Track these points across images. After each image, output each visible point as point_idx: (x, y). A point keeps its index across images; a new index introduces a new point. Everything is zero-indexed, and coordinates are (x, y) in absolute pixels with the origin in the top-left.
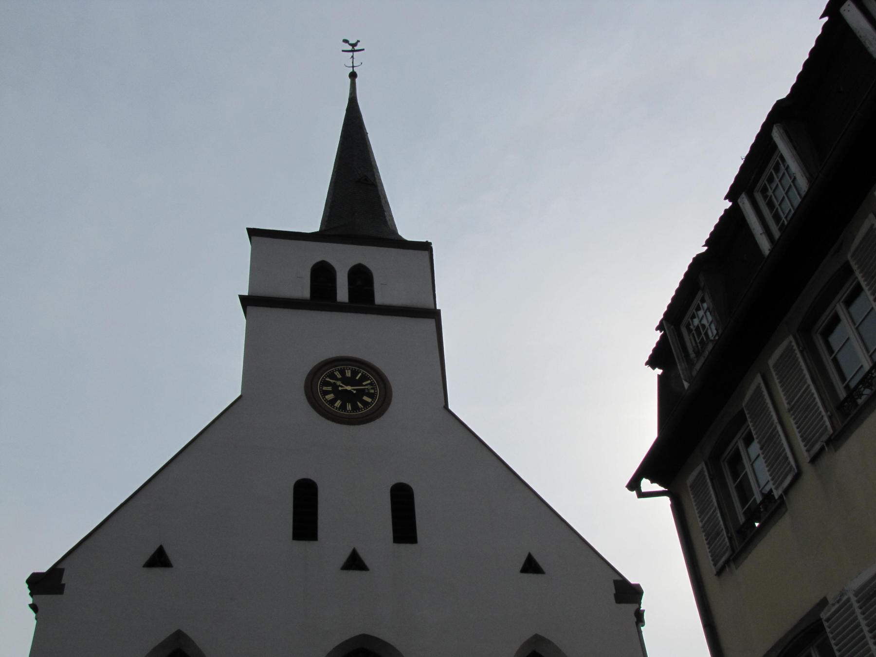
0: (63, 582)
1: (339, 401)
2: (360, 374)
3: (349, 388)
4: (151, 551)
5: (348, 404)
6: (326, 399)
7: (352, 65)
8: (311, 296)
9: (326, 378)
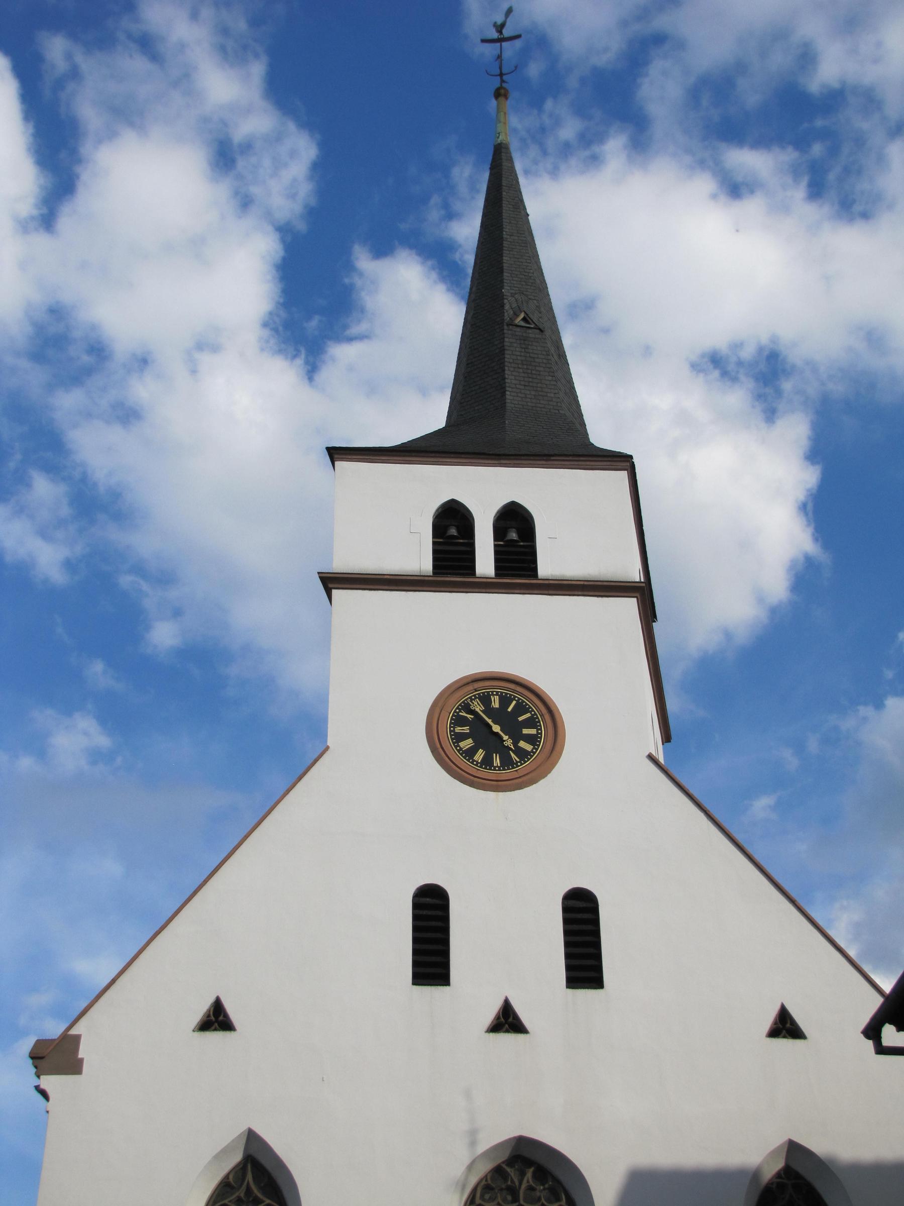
0: (80, 1056)
1: (481, 751)
2: (514, 703)
4: (202, 1007)
5: (494, 755)
6: (461, 749)
7: (498, 72)
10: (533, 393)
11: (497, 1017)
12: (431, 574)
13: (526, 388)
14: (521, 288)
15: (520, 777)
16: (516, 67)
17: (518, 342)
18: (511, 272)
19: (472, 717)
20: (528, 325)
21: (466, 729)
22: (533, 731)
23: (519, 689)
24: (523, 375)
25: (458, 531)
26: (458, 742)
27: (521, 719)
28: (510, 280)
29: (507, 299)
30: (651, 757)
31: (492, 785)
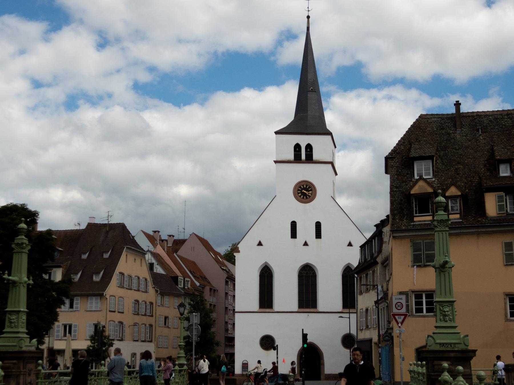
3: (305, 192)
8: (294, 157)
21: (299, 192)
25: (299, 149)
27: (309, 189)
30: (332, 197)
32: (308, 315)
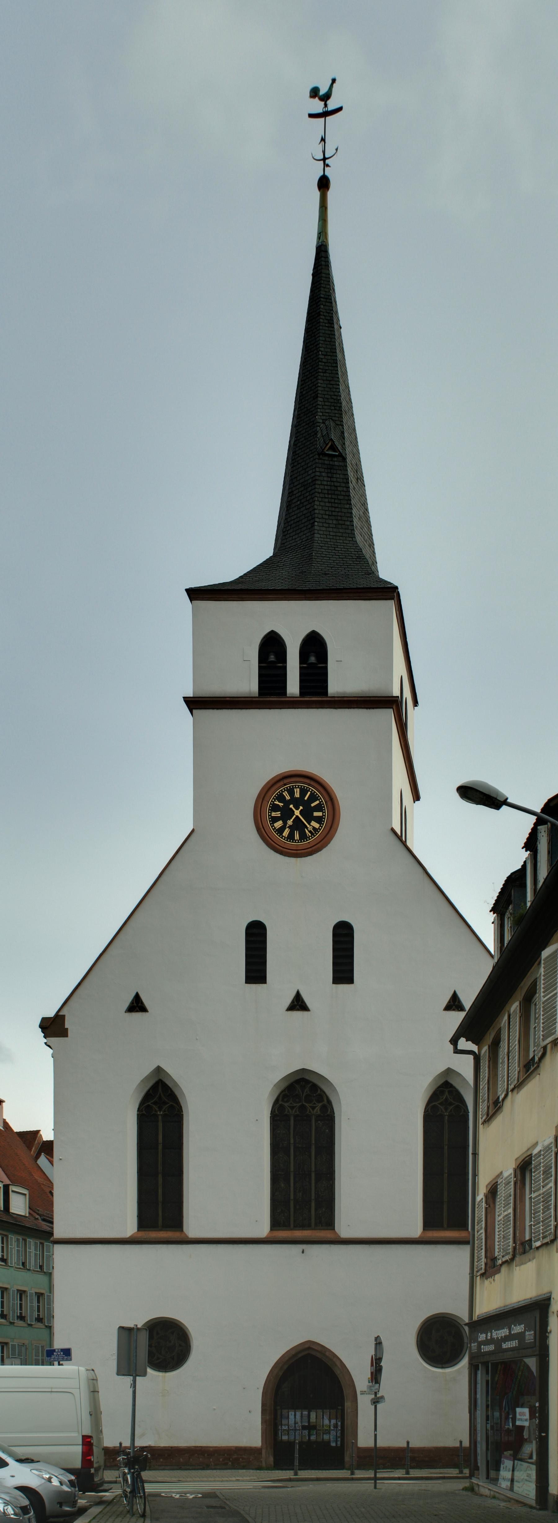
2: (309, 793)
3: (297, 813)
6: (275, 828)
7: (322, 157)
9: (275, 801)
10: (335, 522)
11: (293, 1002)
12: (257, 696)
13: (330, 518)
14: (331, 413)
15: (311, 847)
16: (337, 150)
17: (326, 471)
18: (323, 396)
19: (282, 804)
20: (334, 453)
22: (320, 814)
23: (312, 783)
24: (327, 504)
26: (273, 823)
27: (313, 805)
28: (323, 406)
29: (319, 426)
31: (293, 853)
32: (303, 1252)
